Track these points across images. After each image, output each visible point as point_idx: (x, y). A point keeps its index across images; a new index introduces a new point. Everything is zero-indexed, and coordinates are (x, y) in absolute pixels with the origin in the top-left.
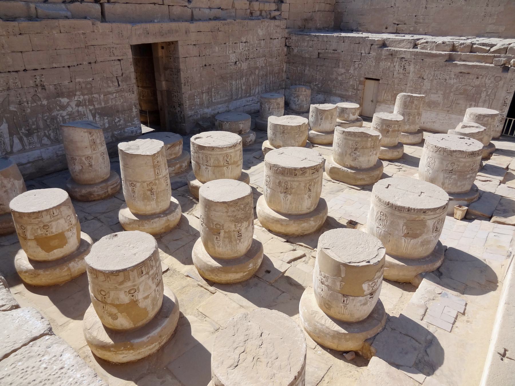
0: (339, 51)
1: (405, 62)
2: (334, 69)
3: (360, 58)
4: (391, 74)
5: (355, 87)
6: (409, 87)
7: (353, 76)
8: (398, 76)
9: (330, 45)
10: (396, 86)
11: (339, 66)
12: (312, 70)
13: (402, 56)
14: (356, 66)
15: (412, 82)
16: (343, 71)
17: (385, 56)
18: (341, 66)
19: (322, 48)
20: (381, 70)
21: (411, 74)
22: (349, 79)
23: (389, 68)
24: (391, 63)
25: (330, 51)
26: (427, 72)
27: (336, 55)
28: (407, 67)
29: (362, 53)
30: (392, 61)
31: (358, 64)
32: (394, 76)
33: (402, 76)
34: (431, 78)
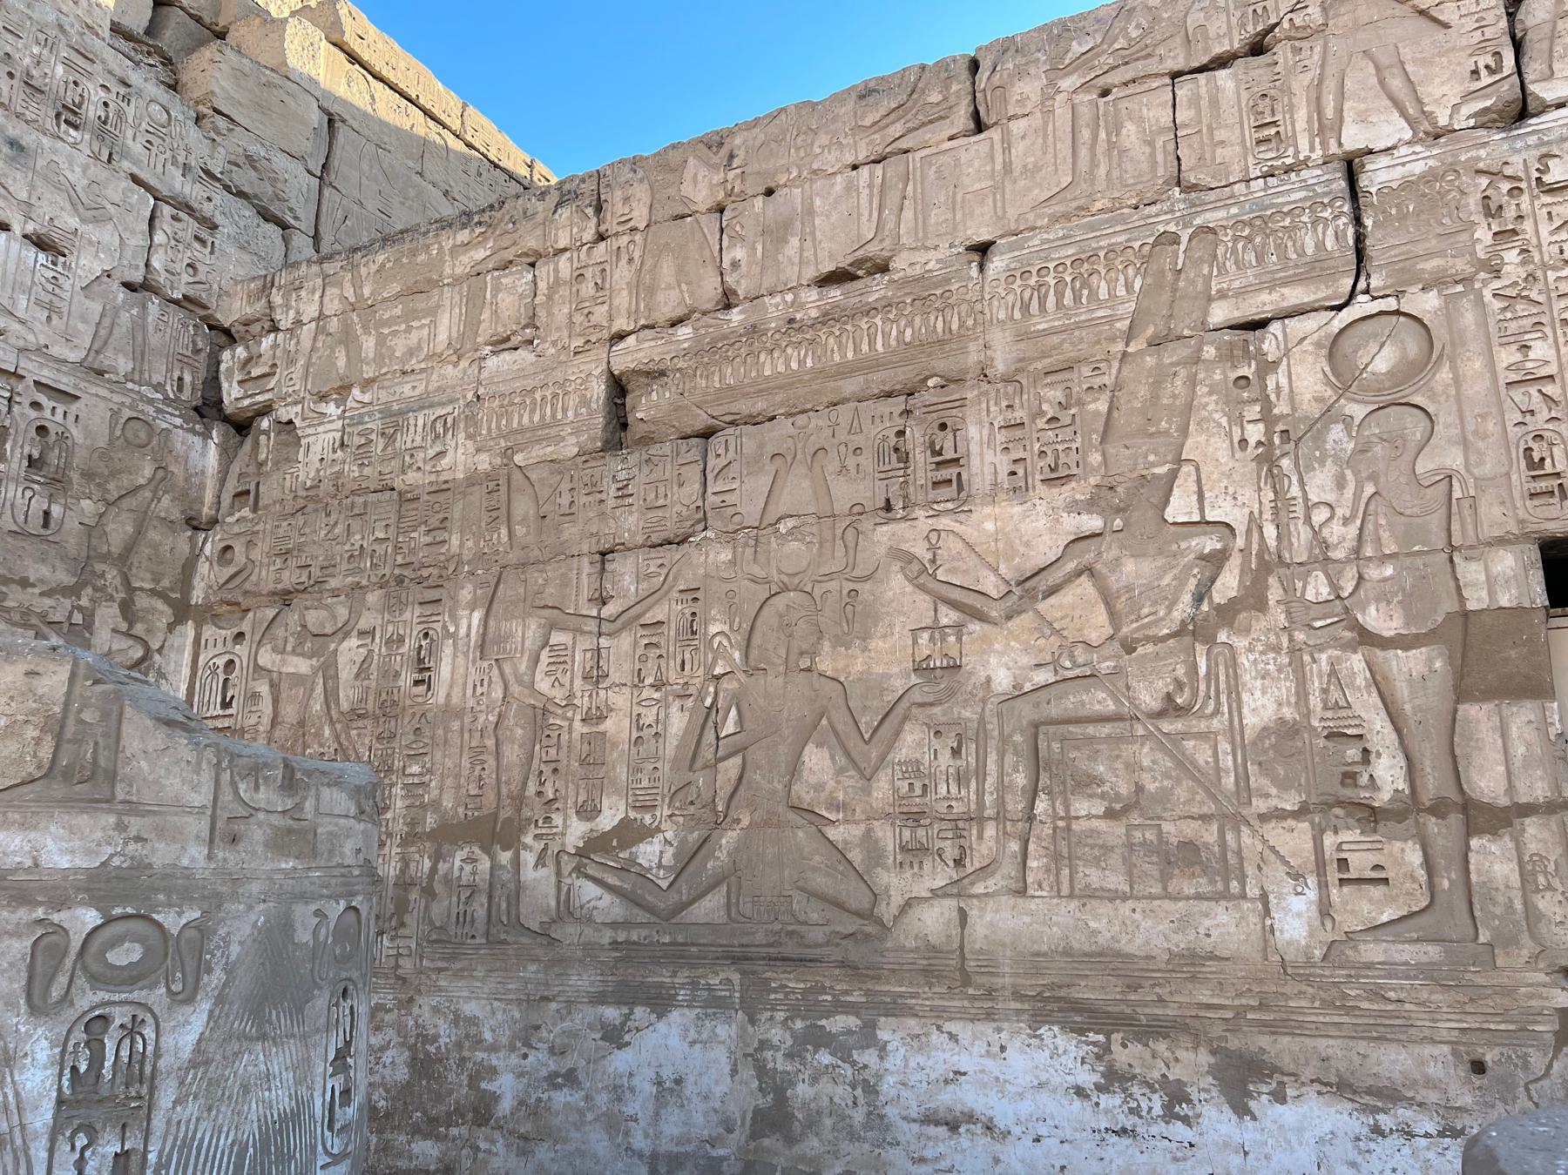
0: (931, 261)
2: (884, 535)
3: (1335, 235)
5: (1388, 775)
7: (1265, 566)
9: (776, 234)
11: (949, 474)
12: (526, 632)
14: (1304, 381)
16: (1039, 527)
18: (985, 459)
19: (668, 303)
22: (1196, 631)
25: (775, 308)
27: (883, 336)
29: (1351, 168)
31: (1334, 347)
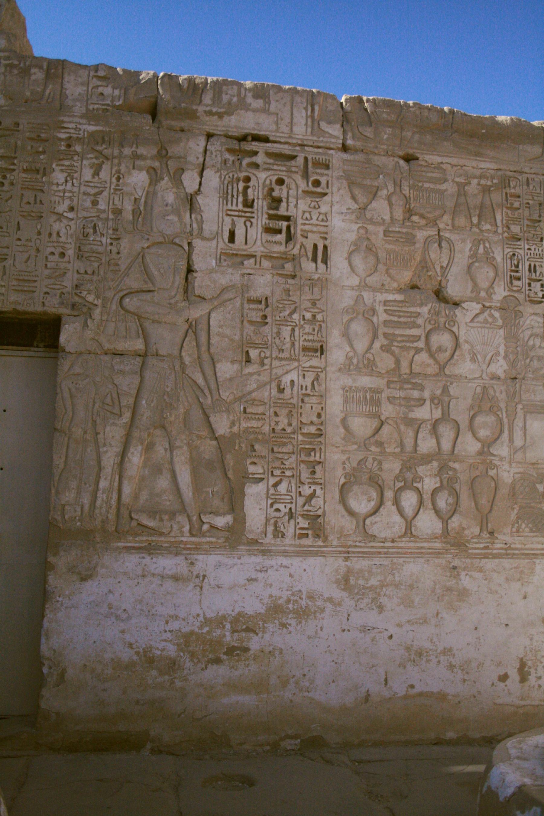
1: (280, 170)
4: (165, 268)
6: (347, 368)
8: (230, 277)
10: (226, 369)
13: (246, 122)
15: (358, 328)
17: (90, 116)
20: (65, 230)
21: (338, 259)
23: (143, 212)
24: (155, 177)
26: (464, 249)
28: (297, 207)
30: (163, 155)
32: (201, 283)
33: (264, 283)
34: (500, 292)
